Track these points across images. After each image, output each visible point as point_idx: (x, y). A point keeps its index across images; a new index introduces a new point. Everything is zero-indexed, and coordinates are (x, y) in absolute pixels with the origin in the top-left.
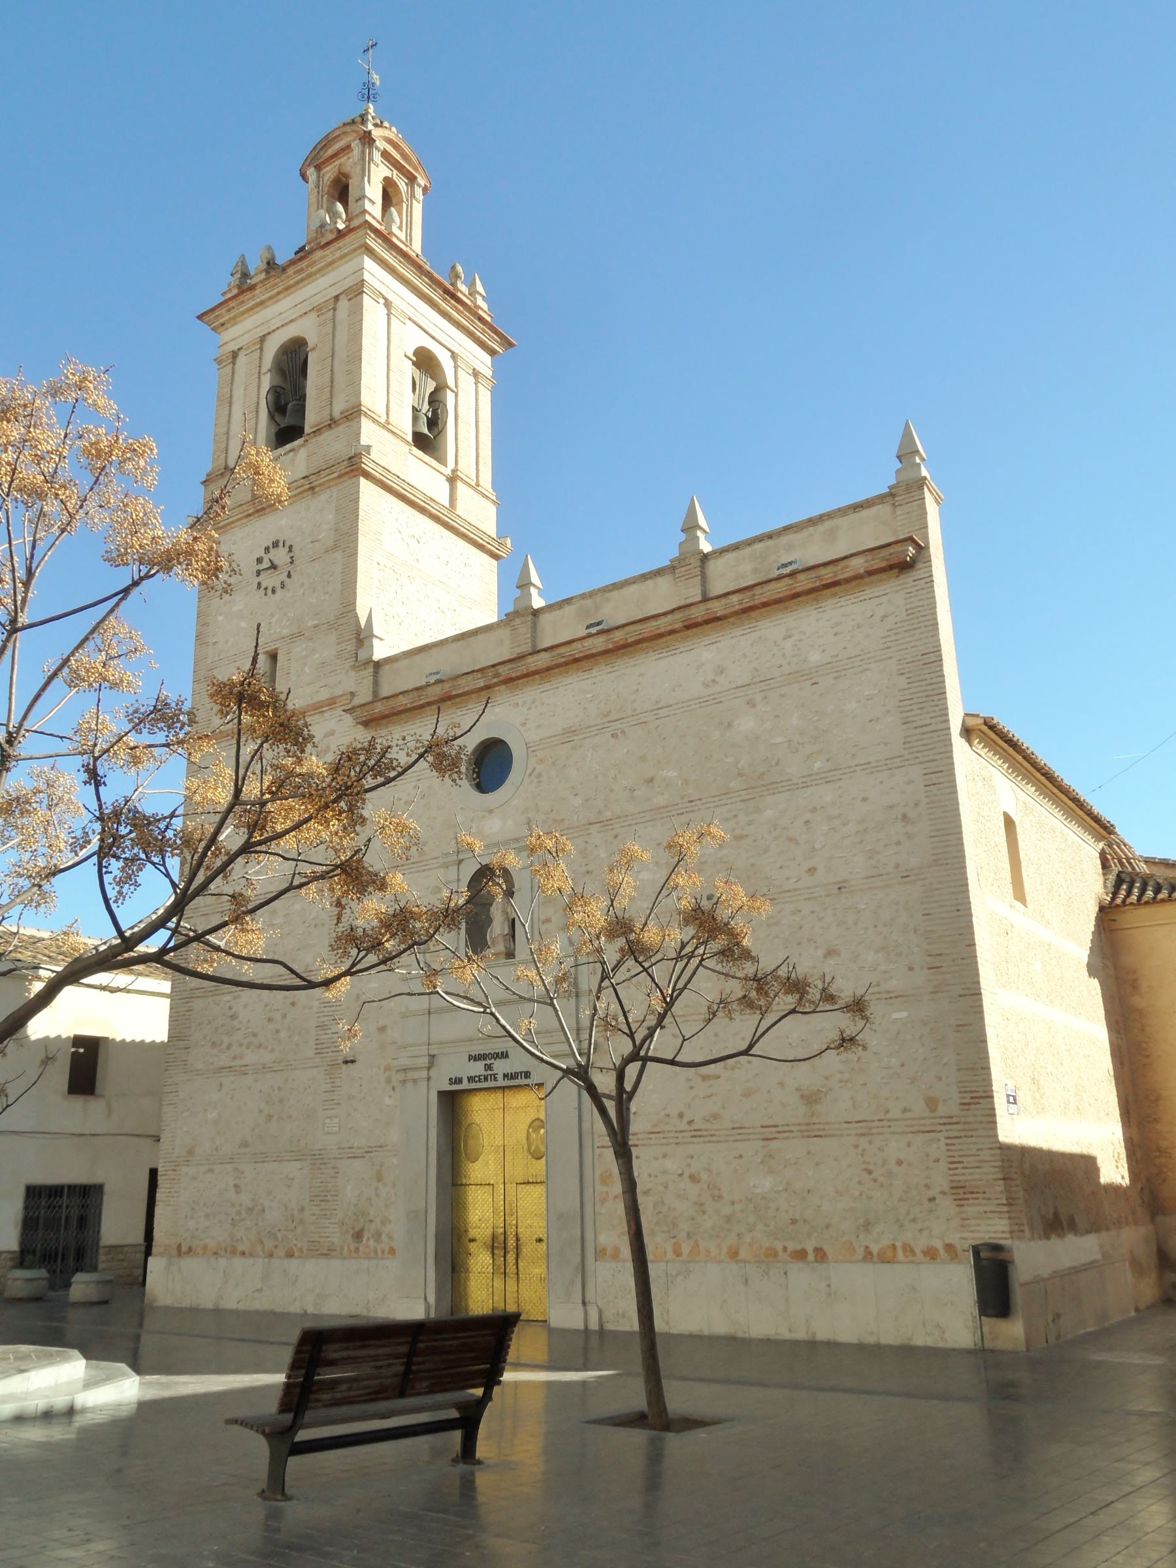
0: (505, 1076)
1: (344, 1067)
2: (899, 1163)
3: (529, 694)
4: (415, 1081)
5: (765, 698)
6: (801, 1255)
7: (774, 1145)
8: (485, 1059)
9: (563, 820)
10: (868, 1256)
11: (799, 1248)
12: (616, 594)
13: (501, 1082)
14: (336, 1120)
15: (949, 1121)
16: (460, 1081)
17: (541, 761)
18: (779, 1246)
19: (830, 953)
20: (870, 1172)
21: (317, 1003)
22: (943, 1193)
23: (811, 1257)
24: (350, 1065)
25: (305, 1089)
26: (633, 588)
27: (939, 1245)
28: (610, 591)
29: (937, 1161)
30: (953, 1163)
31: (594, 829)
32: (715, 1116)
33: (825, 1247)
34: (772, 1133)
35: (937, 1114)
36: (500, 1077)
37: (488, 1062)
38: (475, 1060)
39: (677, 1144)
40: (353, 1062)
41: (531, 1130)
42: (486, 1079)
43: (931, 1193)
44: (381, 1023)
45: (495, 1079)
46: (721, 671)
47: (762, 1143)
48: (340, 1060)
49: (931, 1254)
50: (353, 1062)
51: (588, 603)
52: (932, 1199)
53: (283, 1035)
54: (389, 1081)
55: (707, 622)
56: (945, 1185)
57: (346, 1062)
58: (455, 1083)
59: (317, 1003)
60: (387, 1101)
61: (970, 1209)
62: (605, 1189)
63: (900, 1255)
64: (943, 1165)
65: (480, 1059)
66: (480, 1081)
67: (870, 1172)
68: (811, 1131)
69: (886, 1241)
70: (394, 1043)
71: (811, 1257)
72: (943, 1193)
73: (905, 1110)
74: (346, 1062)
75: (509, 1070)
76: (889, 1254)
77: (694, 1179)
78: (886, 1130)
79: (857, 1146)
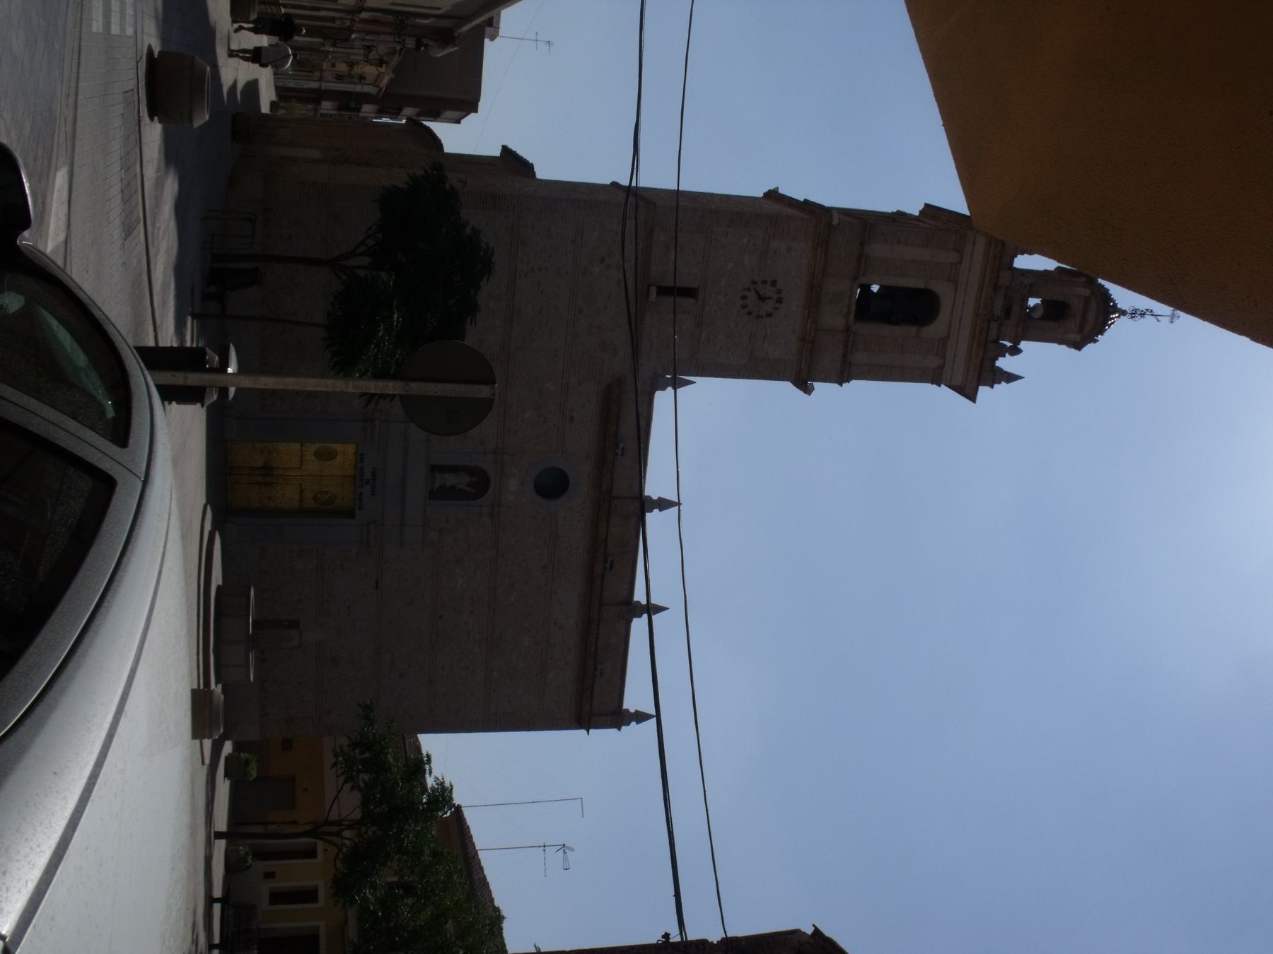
41: (330, 494)
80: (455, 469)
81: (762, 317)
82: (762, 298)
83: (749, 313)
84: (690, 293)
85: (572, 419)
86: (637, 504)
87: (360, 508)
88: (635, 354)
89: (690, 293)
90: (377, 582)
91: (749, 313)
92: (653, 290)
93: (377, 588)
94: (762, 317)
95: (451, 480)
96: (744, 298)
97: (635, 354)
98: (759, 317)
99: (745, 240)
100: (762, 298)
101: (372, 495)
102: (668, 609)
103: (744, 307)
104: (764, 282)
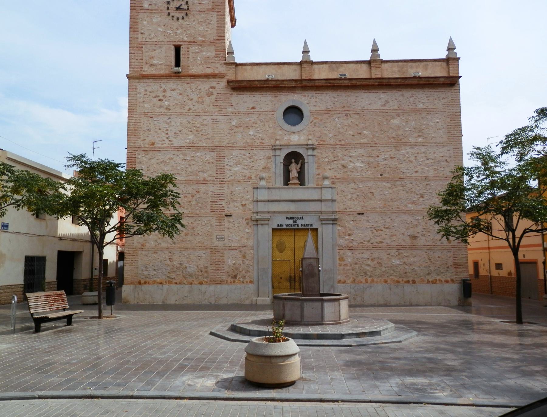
0: (302, 225)
1: (226, 217)
2: (439, 257)
3: (309, 94)
4: (262, 224)
5: (403, 115)
6: (408, 282)
7: (400, 251)
8: (293, 219)
9: (324, 141)
10: (428, 282)
11: (407, 280)
12: (345, 65)
13: (300, 227)
14: (223, 236)
15: (454, 247)
16: (282, 226)
17: (316, 118)
18: (400, 280)
19: (422, 196)
20: (430, 259)
21: (211, 193)
22: (451, 266)
23: (411, 282)
24: (229, 217)
25: (206, 224)
26: (352, 65)
27: (449, 279)
28: (343, 63)
29: (450, 257)
30: (455, 258)
31: (338, 146)
32: (381, 242)
33: (415, 280)
34: (399, 248)
35: (451, 244)
36: (300, 225)
37: (295, 220)
38: (289, 219)
39: (368, 250)
40: (230, 216)
42: (294, 225)
43: (447, 266)
44: (243, 203)
45: (298, 226)
46: (387, 102)
47: (396, 250)
48: (224, 214)
49: (447, 282)
50: (230, 216)
51: (334, 65)
52: (448, 267)
53: (193, 203)
54: (247, 224)
55: (386, 85)
56: (452, 264)
57: (227, 216)
58: (280, 226)
59: (211, 193)
60: (247, 230)
61: (458, 270)
62: (341, 263)
63: (438, 282)
64: (451, 258)
65: (291, 219)
66: (291, 226)
67: (430, 259)
68: (413, 248)
69: (433, 278)
70: (250, 210)
71: (411, 282)
72: (451, 266)
73: (441, 243)
74: (227, 216)
75: (303, 223)
76: (435, 281)
77: (373, 260)
78: (436, 248)
79: (426, 252)
80: (287, 173)
81: (188, 7)
82: (178, 8)
83: (187, 15)
84: (178, 49)
85: (253, 108)
86: (305, 65)
87: (311, 225)
88: (214, 76)
89: (178, 49)
90: (359, 214)
91: (187, 15)
92: (177, 69)
93: (363, 214)
94: (188, 7)
95: (294, 173)
96: (178, 19)
97: (214, 76)
98: (188, 9)
99: (145, 23)
100: (178, 8)
101: (303, 219)
102: (374, 39)
103: (183, 18)
104: (168, 9)
